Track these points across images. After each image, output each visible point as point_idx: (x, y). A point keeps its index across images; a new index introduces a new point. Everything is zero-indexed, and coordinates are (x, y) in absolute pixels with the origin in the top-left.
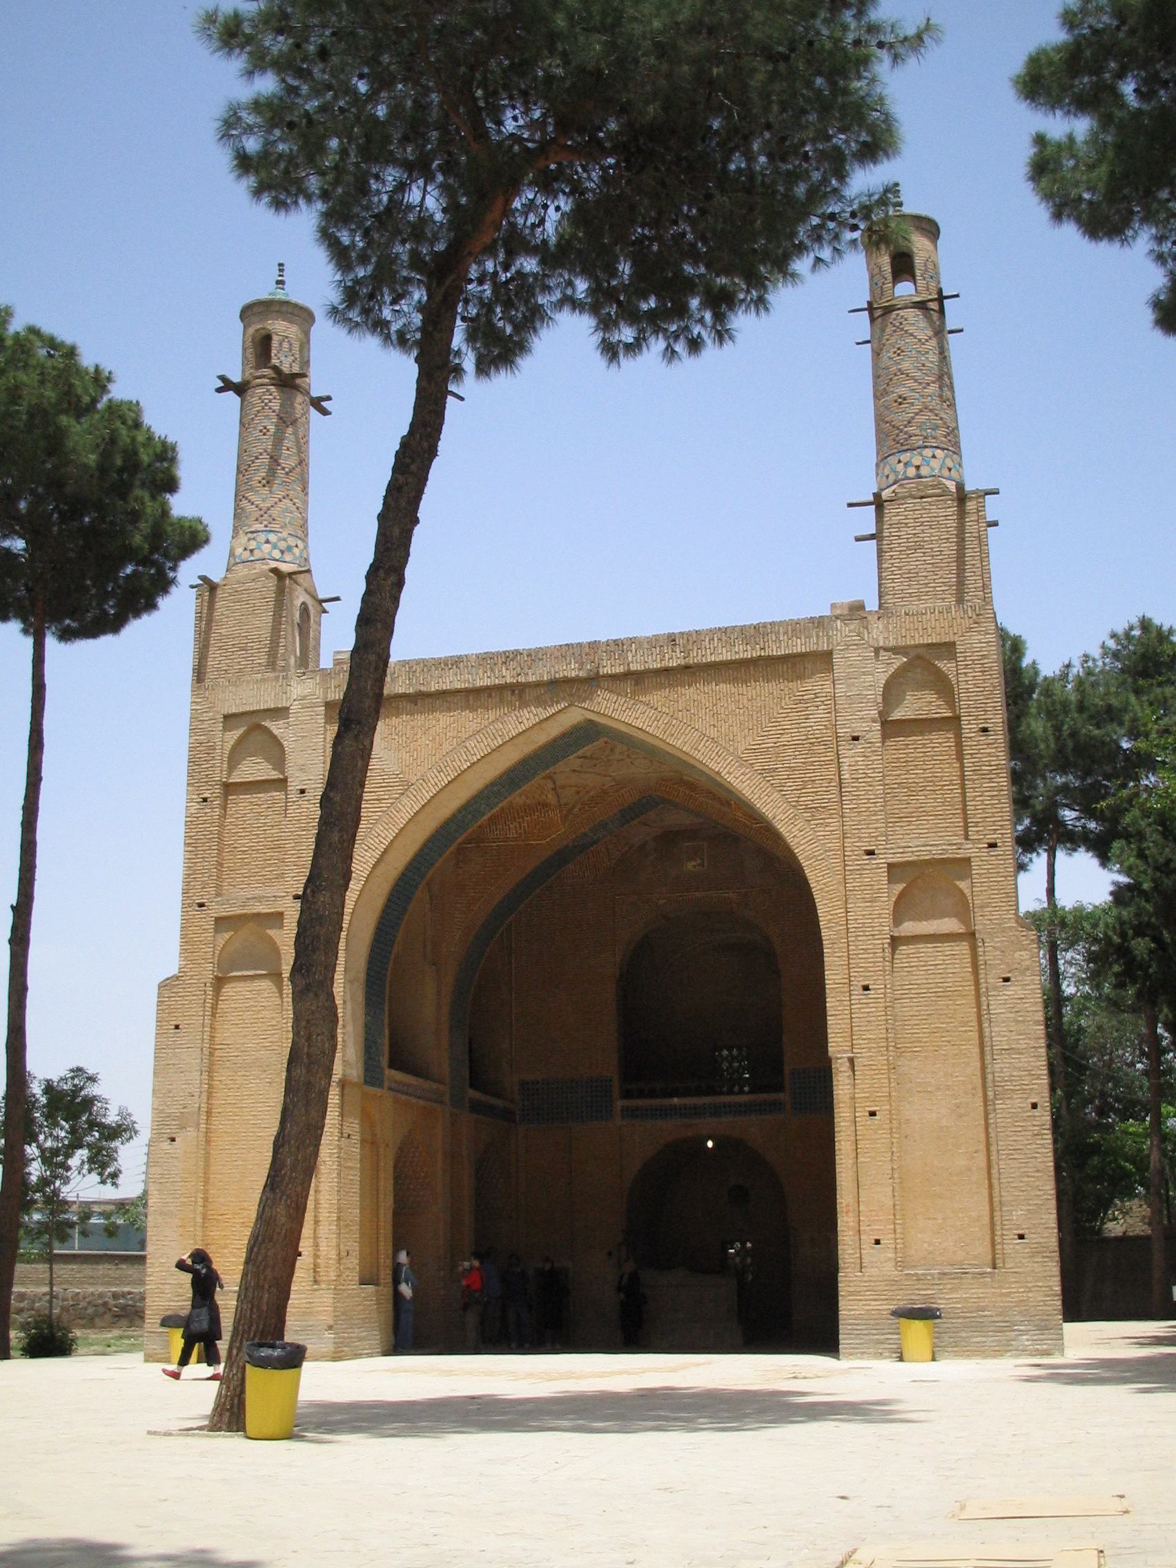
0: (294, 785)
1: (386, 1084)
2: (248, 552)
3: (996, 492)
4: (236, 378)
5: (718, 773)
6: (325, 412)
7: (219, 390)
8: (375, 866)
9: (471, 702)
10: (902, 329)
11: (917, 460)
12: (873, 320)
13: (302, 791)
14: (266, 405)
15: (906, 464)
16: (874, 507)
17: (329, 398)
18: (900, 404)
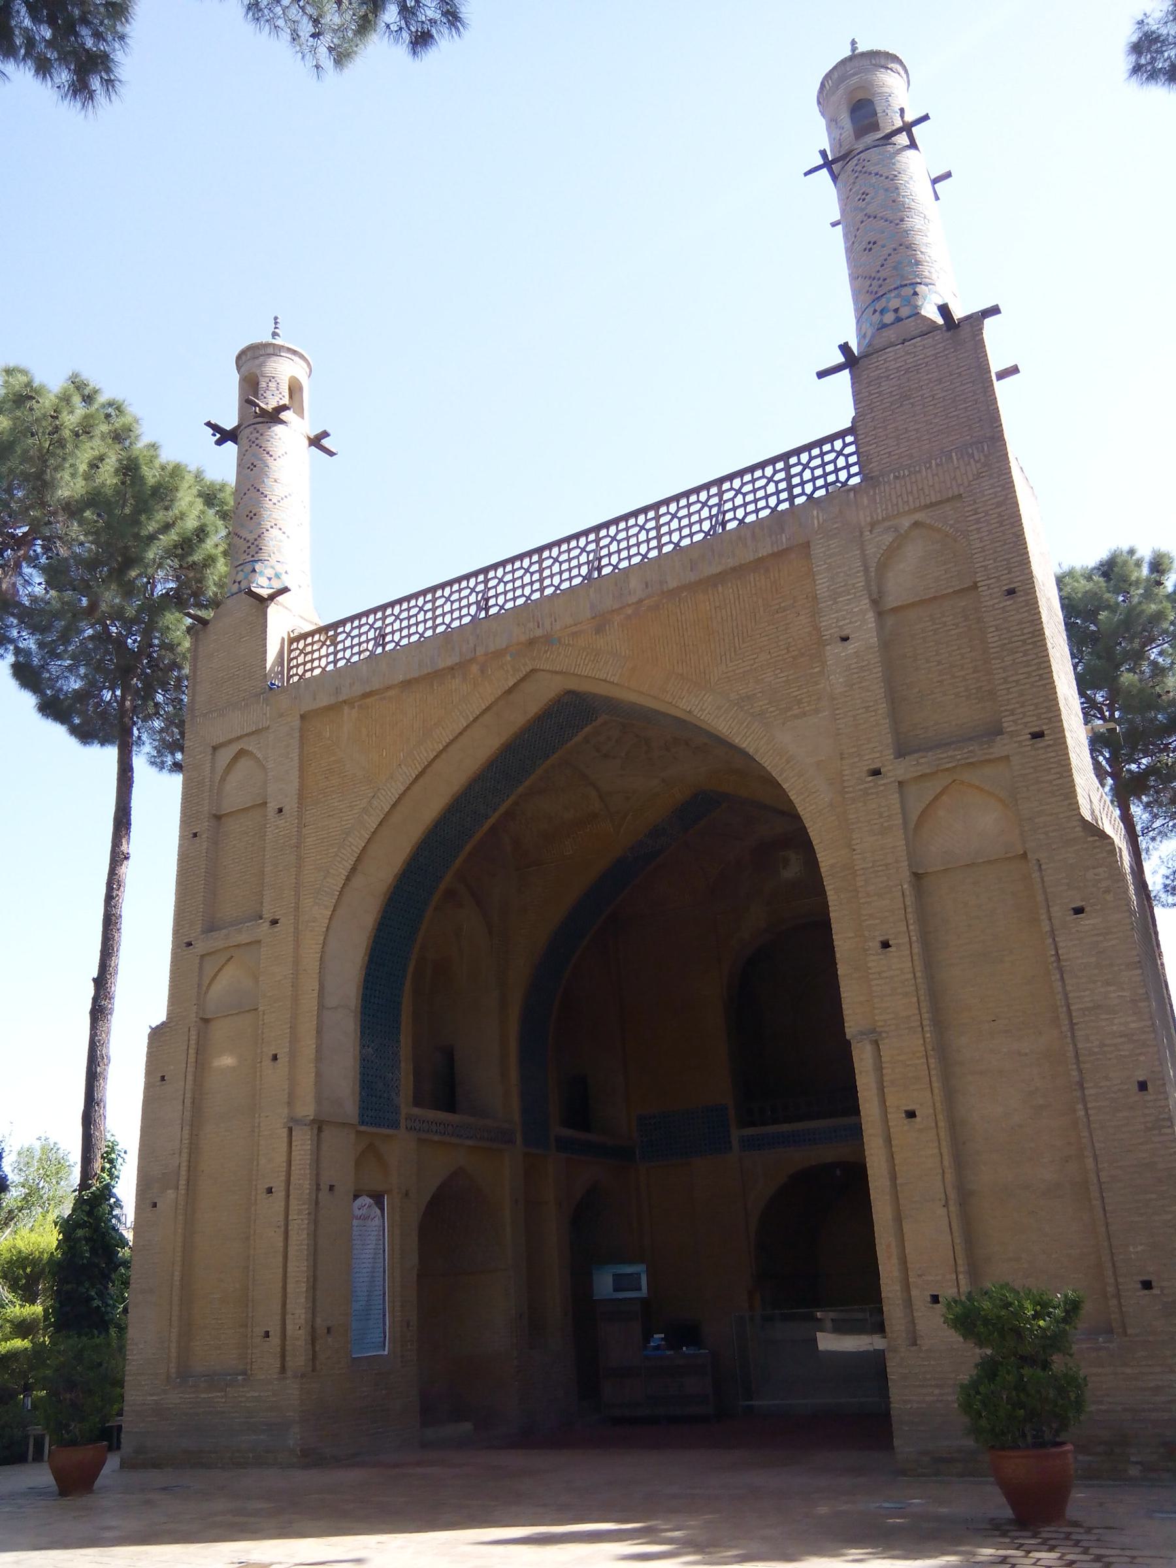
0: (272, 806)
1: (403, 1123)
2: (237, 584)
3: (994, 311)
4: (229, 422)
5: (690, 712)
6: (331, 454)
7: (219, 443)
8: (348, 879)
9: (435, 688)
10: (865, 173)
11: (895, 303)
12: (834, 178)
13: (280, 810)
14: (253, 442)
15: (882, 312)
16: (847, 371)
17: (325, 434)
18: (870, 250)
